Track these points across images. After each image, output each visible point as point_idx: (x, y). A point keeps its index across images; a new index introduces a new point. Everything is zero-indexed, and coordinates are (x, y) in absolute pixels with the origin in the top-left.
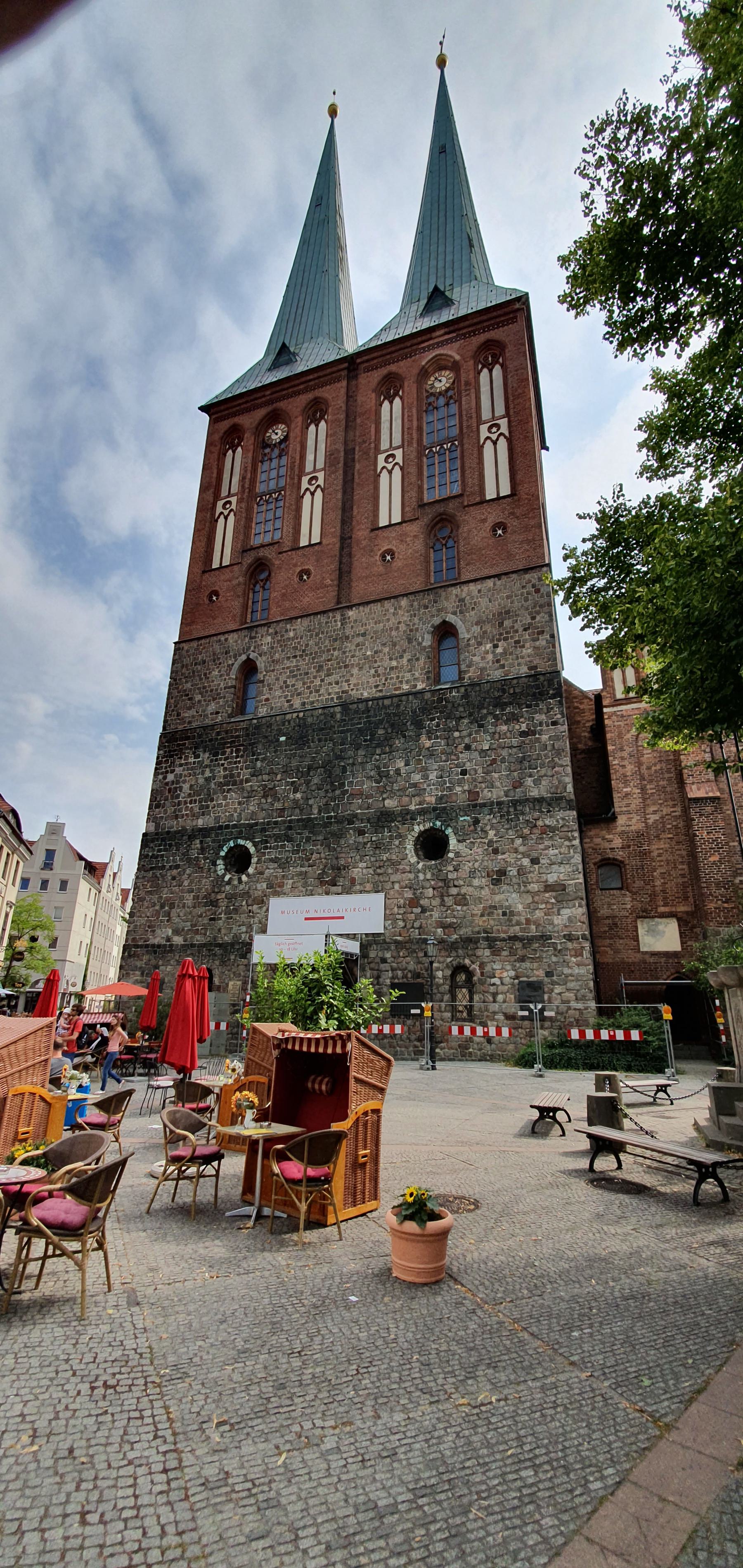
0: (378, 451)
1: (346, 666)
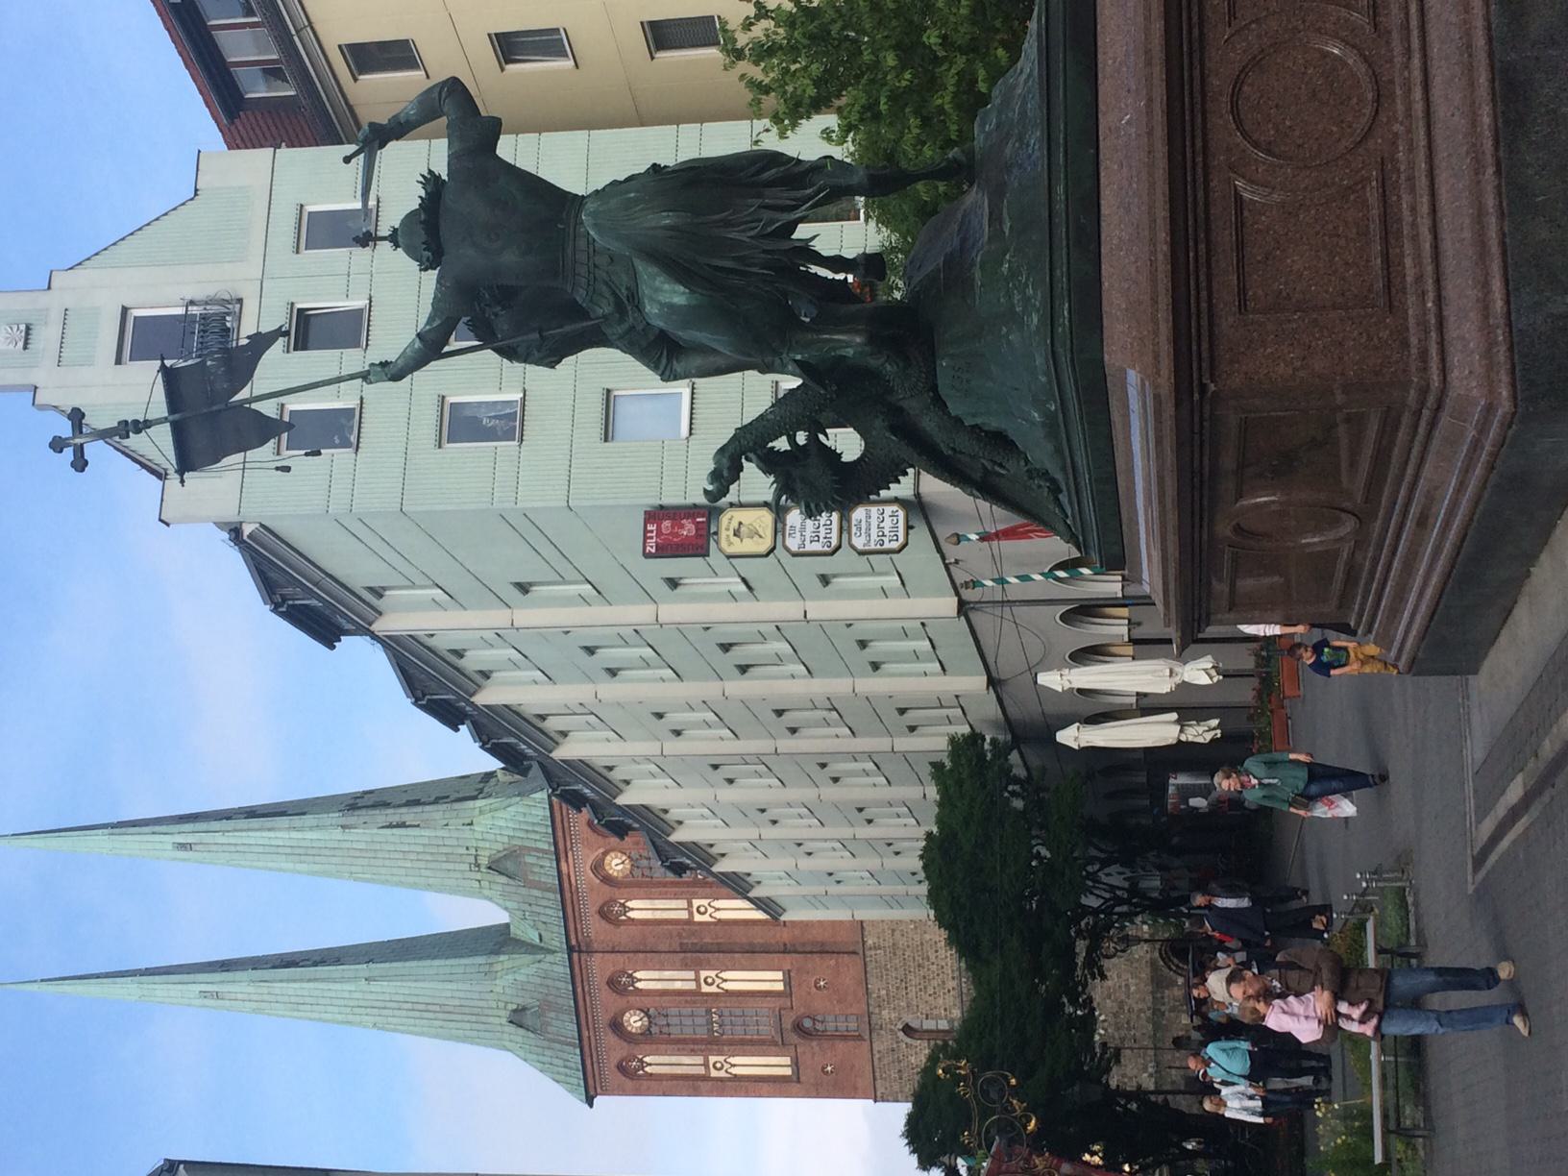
0: (690, 922)
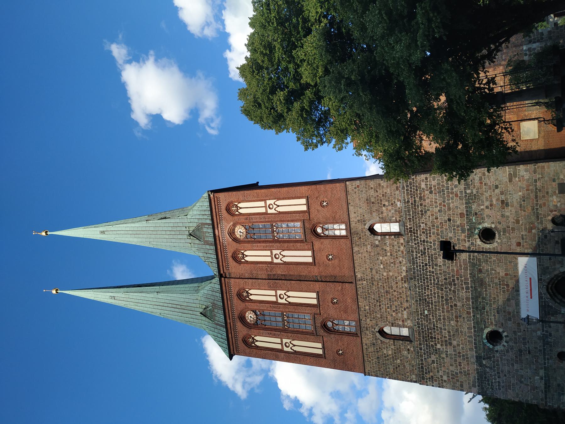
1: (388, 278)
